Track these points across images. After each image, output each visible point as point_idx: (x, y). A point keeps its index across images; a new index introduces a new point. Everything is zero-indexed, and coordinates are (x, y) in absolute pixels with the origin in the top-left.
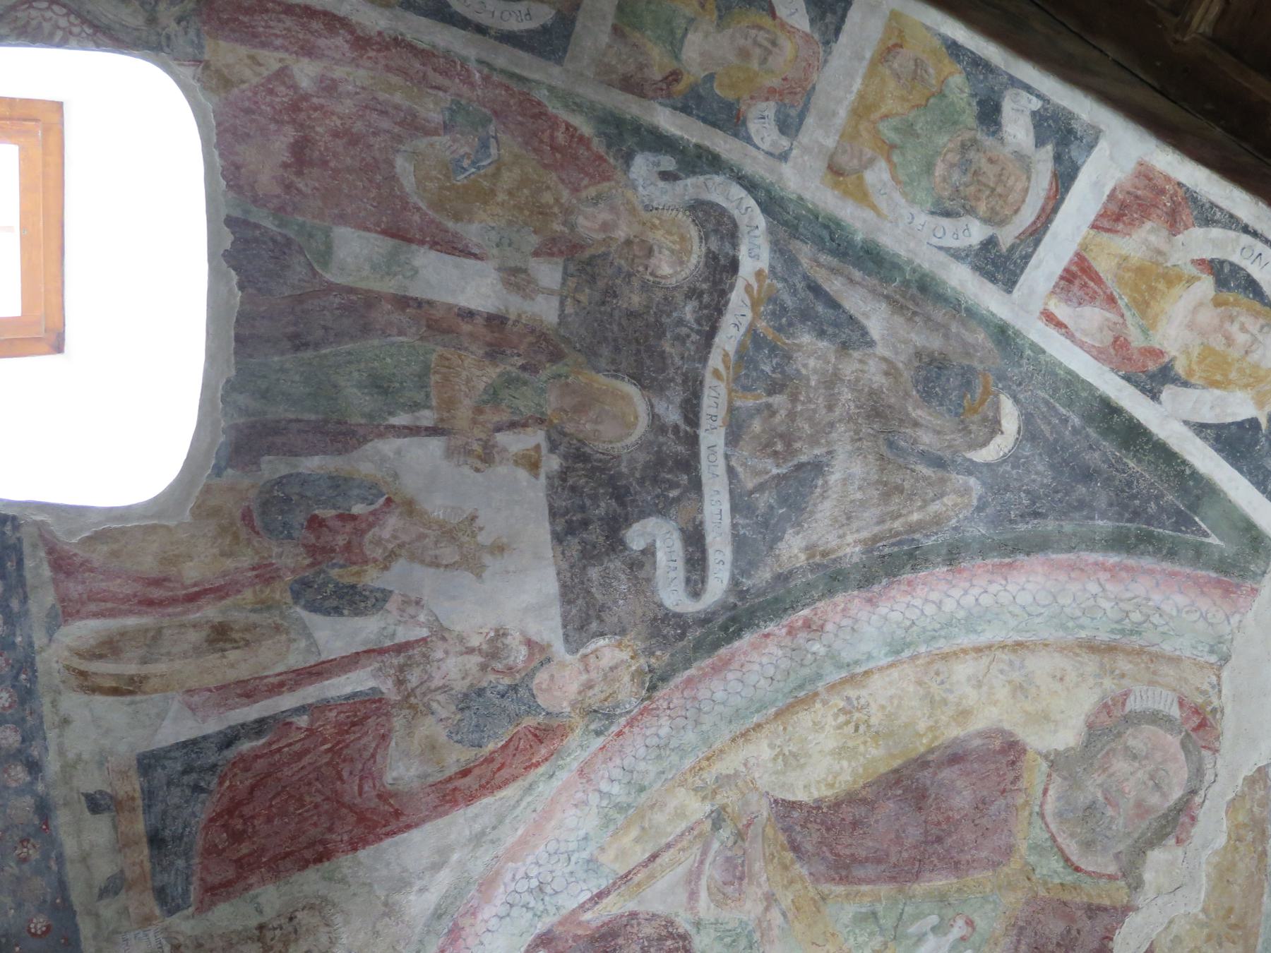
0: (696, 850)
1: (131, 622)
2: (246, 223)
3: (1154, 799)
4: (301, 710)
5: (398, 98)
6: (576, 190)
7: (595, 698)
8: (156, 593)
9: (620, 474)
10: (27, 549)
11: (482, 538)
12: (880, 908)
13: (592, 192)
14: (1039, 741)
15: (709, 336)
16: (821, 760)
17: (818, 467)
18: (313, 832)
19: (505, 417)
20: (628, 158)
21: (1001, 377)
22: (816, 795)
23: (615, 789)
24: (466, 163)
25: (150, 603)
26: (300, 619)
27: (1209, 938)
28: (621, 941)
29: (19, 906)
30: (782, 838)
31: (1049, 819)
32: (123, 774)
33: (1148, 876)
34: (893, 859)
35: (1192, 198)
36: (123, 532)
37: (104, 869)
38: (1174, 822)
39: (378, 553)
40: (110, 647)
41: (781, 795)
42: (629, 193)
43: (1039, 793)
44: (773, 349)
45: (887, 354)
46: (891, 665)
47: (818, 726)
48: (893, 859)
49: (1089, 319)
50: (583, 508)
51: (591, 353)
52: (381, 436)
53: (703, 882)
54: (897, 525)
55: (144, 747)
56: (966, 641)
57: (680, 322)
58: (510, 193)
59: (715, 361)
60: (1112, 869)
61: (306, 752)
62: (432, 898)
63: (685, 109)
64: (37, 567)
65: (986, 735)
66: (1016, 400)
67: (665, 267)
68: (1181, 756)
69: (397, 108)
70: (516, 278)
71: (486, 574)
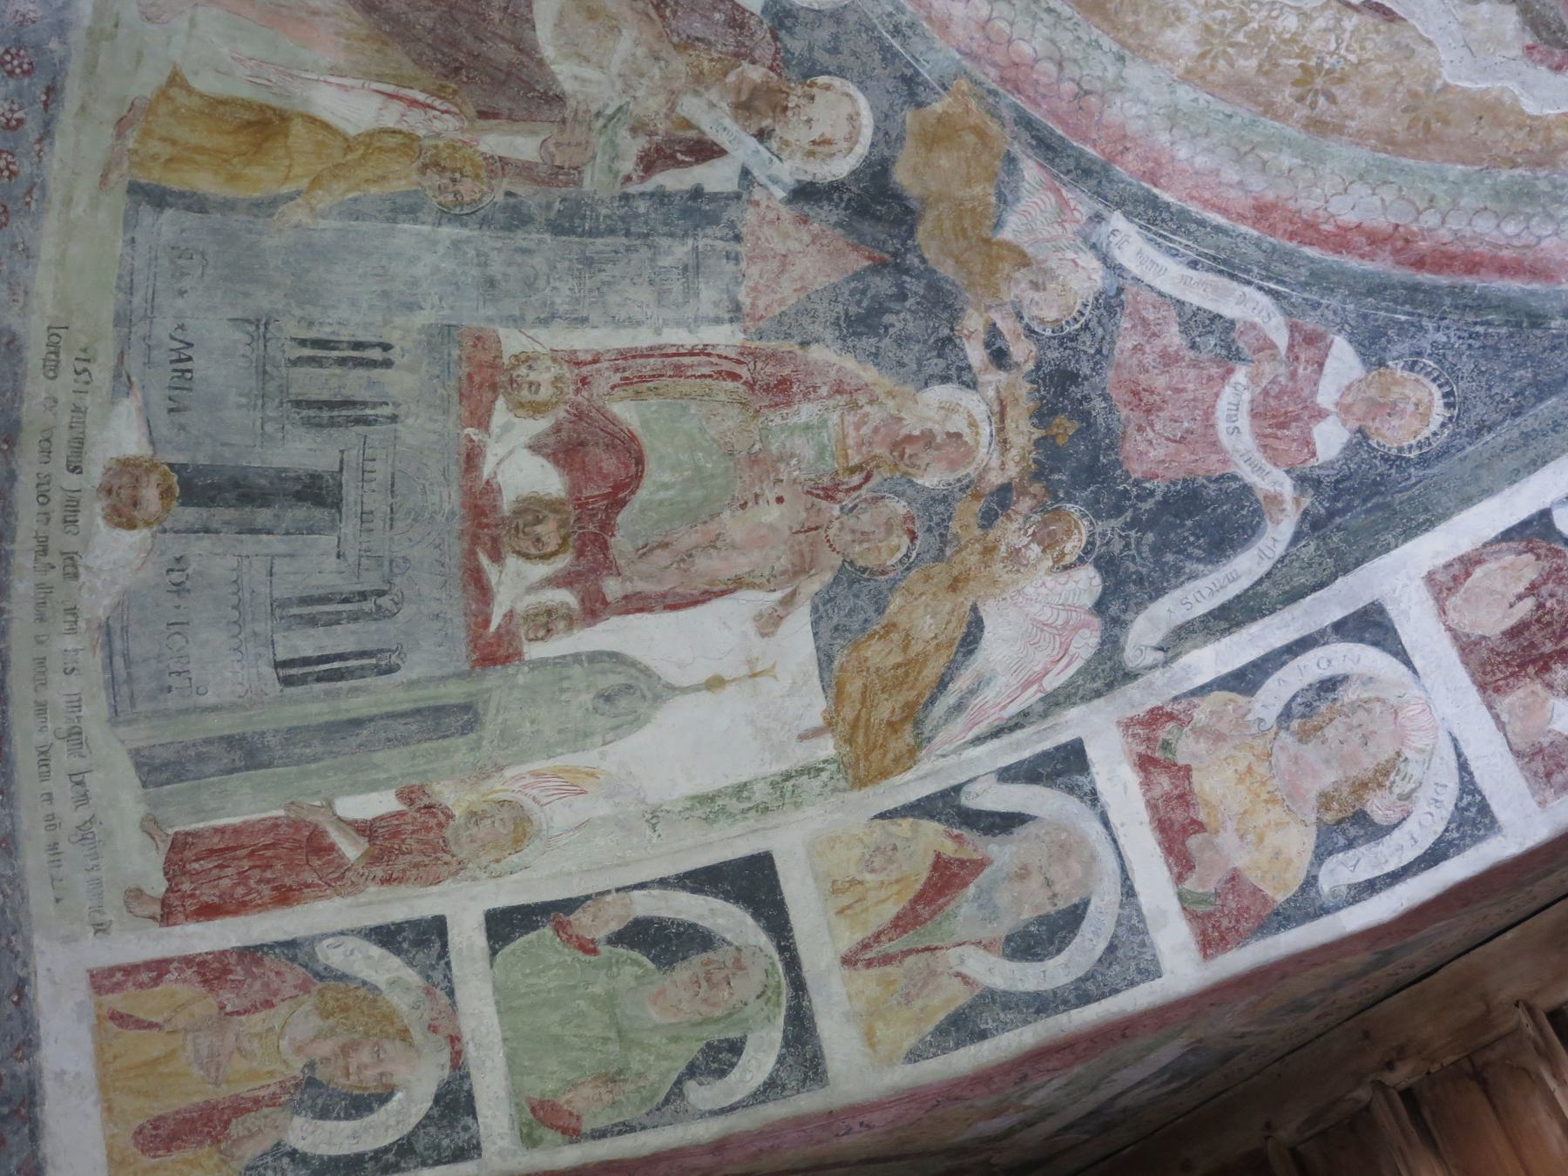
27: (1414, 95)
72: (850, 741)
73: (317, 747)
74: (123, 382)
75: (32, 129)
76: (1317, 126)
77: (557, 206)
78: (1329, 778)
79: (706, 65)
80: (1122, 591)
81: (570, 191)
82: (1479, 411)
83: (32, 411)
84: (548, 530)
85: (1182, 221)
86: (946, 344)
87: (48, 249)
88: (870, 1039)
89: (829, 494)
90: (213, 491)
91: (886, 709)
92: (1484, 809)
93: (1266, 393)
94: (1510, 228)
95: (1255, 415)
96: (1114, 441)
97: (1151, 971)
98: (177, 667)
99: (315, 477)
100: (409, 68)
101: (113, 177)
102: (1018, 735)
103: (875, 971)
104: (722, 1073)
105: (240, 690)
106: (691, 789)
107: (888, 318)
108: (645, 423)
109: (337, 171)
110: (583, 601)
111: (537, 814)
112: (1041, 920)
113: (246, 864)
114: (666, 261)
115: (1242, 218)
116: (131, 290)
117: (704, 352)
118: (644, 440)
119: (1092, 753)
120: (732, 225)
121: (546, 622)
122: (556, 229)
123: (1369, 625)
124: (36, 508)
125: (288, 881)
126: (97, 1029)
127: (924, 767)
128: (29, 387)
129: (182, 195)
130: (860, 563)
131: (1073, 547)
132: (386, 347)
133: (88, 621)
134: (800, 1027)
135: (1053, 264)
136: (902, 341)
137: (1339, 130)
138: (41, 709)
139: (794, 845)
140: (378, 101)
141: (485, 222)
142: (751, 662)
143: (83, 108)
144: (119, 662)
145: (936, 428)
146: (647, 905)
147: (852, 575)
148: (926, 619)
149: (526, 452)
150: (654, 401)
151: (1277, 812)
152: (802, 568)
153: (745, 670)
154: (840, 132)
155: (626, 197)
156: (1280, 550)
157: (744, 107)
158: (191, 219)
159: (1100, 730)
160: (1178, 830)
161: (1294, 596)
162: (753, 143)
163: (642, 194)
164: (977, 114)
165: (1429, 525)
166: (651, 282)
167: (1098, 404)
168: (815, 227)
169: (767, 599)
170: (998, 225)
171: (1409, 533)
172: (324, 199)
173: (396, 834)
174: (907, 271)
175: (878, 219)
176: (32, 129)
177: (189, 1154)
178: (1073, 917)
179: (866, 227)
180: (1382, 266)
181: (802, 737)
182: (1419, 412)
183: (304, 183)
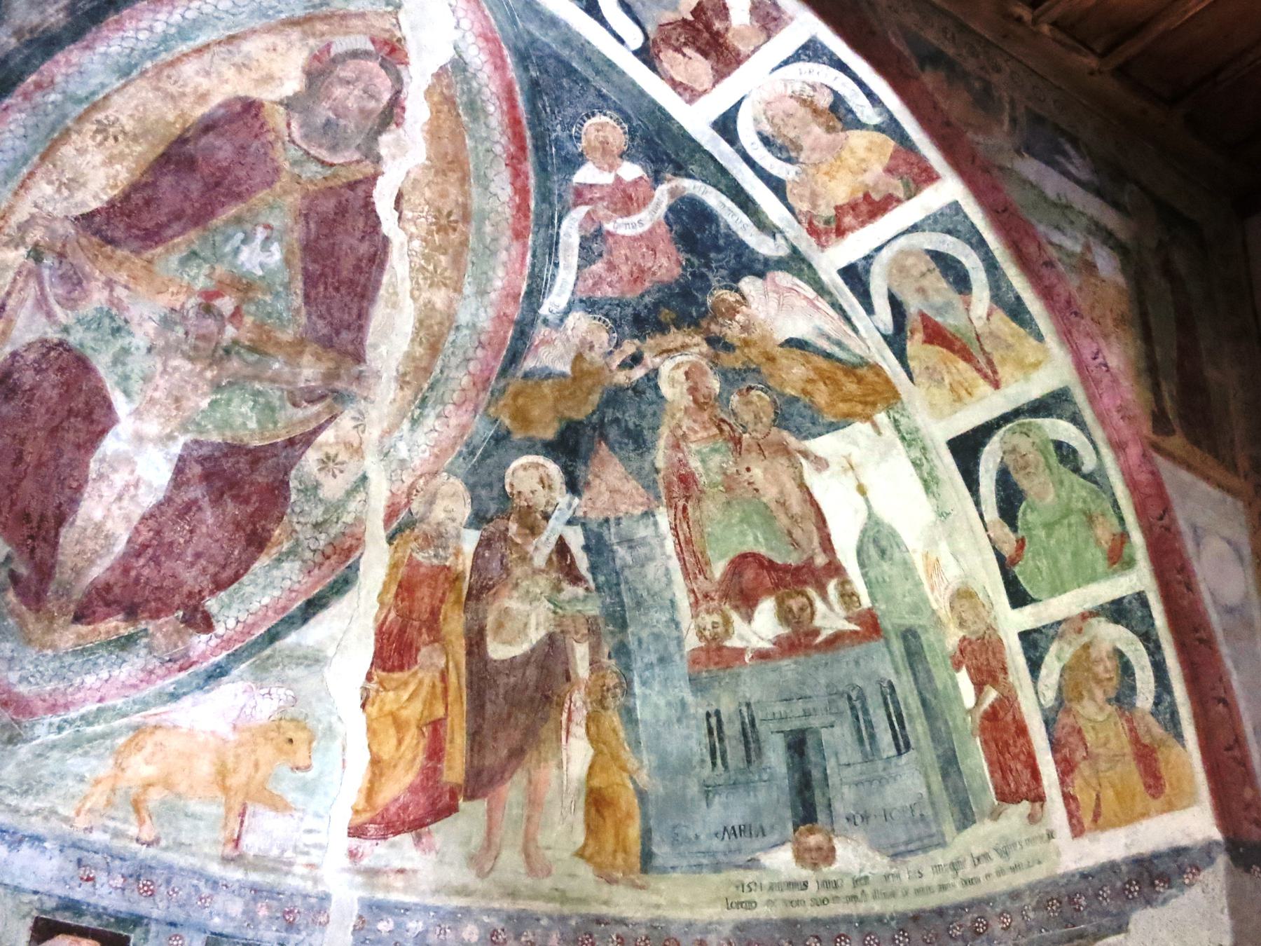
0: (33, 284)
3: (372, 104)
12: (195, 247)
14: (267, 95)
22: (106, 198)
27: (437, 173)
28: (16, 376)
30: (95, 239)
31: (299, 141)
33: (383, 151)
34: (189, 211)
38: (392, 114)
41: (76, 212)
43: (283, 126)
46: (124, 86)
47: (81, 152)
48: (189, 211)
53: (52, 300)
56: (184, 48)
60: (357, 156)
65: (226, 105)
68: (383, 72)
72: (874, 404)
73: (940, 724)
74: (752, 864)
75: (622, 930)
77: (611, 628)
78: (817, 130)
79: (514, 556)
80: (747, 264)
81: (601, 621)
82: (591, 98)
83: (775, 913)
84: (795, 603)
85: (534, 276)
86: (636, 389)
87: (685, 915)
88: (1036, 365)
89: (738, 442)
90: (807, 804)
91: (851, 387)
92: (805, 47)
93: (615, 211)
94: (491, 109)
95: (629, 214)
96: (664, 287)
97: (955, 207)
98: (909, 814)
99: (789, 747)
100: (551, 724)
101: (639, 882)
102: (845, 307)
103: (999, 370)
104: (1074, 451)
105: (917, 773)
107: (631, 425)
108: (722, 557)
109: (615, 758)
110: (832, 577)
111: (954, 585)
112: (945, 275)
113: (1007, 756)
114: (629, 560)
115: (525, 245)
116: (700, 865)
117: (675, 529)
118: (731, 555)
119: (843, 264)
120: (600, 525)
121: (848, 597)
122: (624, 626)
123: (726, 126)
124: (831, 905)
125: (1013, 729)
126: (1103, 829)
128: (762, 916)
129: (643, 844)
130: (773, 416)
131: (731, 297)
132: (708, 715)
133: (891, 867)
135: (577, 341)
136: (642, 415)
137: (465, 207)
138: (943, 887)
140: (571, 740)
141: (628, 668)
142: (845, 471)
143: (606, 903)
144: (912, 847)
145: (685, 386)
146: (992, 513)
147: (781, 419)
148: (795, 373)
149: (754, 624)
150: (709, 553)
151: (845, 154)
152: (785, 450)
153: (850, 473)
155: (598, 588)
156: (699, 183)
157: (533, 530)
158: (656, 837)
159: (831, 260)
160: (872, 207)
161: (723, 171)
162: (552, 522)
163: (595, 580)
164: (506, 400)
165: (661, 109)
166: (643, 566)
167: (647, 299)
168: (590, 477)
170: (563, 375)
171: (669, 118)
172: (632, 764)
173: (979, 670)
174: (602, 420)
175: (577, 443)
176: (622, 930)
177: (1162, 765)
178: (937, 256)
180: (529, 167)
181: (879, 433)
182: (603, 128)
183: (625, 775)
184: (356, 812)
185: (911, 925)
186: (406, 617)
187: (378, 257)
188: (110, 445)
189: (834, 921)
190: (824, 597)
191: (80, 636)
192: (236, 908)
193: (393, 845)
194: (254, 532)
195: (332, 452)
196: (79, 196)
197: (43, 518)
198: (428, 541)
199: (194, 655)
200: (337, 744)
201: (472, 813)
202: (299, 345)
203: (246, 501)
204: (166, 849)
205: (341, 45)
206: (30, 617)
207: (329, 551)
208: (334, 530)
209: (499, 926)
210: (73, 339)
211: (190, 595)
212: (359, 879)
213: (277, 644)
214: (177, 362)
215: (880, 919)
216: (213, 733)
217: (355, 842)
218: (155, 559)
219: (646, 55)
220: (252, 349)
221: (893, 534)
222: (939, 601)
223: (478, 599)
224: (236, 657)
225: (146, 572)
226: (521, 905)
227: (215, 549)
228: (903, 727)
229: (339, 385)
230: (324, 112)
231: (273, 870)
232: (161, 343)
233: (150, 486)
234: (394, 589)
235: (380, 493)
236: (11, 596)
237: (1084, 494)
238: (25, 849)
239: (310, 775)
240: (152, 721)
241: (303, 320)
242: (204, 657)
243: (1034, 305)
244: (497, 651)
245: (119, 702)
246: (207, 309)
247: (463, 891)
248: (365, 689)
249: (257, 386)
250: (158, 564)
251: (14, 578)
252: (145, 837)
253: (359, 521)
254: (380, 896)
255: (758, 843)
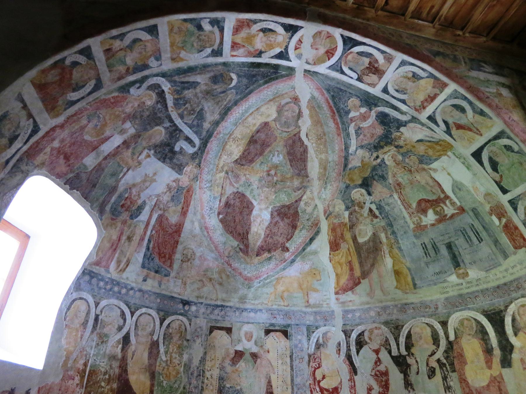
1: (117, 255)
2: (68, 180)
3: (294, 114)
4: (152, 231)
5: (76, 127)
6: (122, 106)
7: (192, 177)
8: (114, 247)
9: (166, 142)
10: (91, 269)
11: (150, 176)
12: (262, 161)
13: (125, 103)
14: (269, 120)
15: (166, 107)
16: (236, 150)
17: (202, 109)
18: (173, 242)
19: (138, 154)
20: (128, 91)
21: (228, 71)
23: (207, 185)
24: (97, 124)
25: (115, 249)
26: (137, 221)
29: (154, 303)
30: (239, 166)
32: (143, 272)
35: (251, 20)
36: (99, 247)
37: (156, 284)
38: (300, 115)
39: (136, 197)
40: (119, 262)
41: (233, 161)
42: (133, 97)
44: (180, 99)
45: (204, 82)
47: (231, 146)
49: (241, 51)
50: (164, 153)
51: (145, 130)
52: (120, 181)
54: (223, 107)
55: (140, 265)
56: (247, 115)
57: (159, 109)
58: (110, 119)
59: (170, 109)
60: (294, 128)
61: (159, 235)
62: (198, 228)
63: (134, 73)
64: (96, 269)
65: (260, 125)
66: (233, 73)
67: (149, 103)
69: (77, 129)
70: (122, 132)
71: (157, 180)
72: (446, 151)
74: (445, 281)
75: (413, 306)
76: (325, 135)
78: (410, 83)
80: (400, 124)
82: (348, 95)
83: (456, 293)
84: (438, 209)
85: (346, 144)
86: (380, 165)
87: (430, 298)
88: (492, 126)
89: (411, 171)
90: (456, 262)
91: (438, 148)
92: (401, 63)
94: (324, 106)
95: (366, 121)
97: (456, 91)
99: (447, 247)
100: (380, 256)
104: (511, 147)
106: (467, 171)
108: (414, 202)
111: (484, 193)
112: (457, 110)
114: (389, 209)
116: (430, 284)
117: (399, 198)
118: (417, 201)
119: (427, 116)
121: (453, 204)
122: (392, 226)
123: (385, 90)
127: (445, 139)
131: (398, 134)
132: (422, 244)
134: (497, 137)
135: (361, 157)
138: (504, 277)
139: (468, 151)
141: (396, 237)
146: (489, 170)
147: (421, 162)
148: (421, 149)
150: (410, 202)
152: (424, 169)
154: (359, 194)
155: (383, 218)
157: (362, 208)
158: (416, 279)
159: (423, 116)
160: (432, 98)
161: (387, 102)
164: (346, 176)
165: (367, 92)
167: (376, 141)
169: (432, 172)
170: (360, 167)
171: (369, 93)
172: (404, 261)
173: (498, 214)
175: (367, 182)
178: (454, 106)
179: (369, 183)
182: (353, 101)
184: (335, 288)
185: (497, 290)
186: (335, 237)
187: (305, 151)
188: (254, 213)
189: (474, 292)
190: (446, 205)
191: (259, 260)
192: (312, 318)
193: (347, 295)
194: (293, 225)
195: (307, 201)
196: (233, 156)
197: (243, 233)
198: (336, 217)
199: (286, 258)
200: (326, 272)
201: (365, 283)
202: (292, 178)
203: (289, 218)
204: (291, 307)
205: (283, 102)
206: (246, 257)
207: (312, 225)
208: (312, 220)
209: (379, 310)
210: (240, 190)
211: (282, 244)
212: (340, 305)
213: (305, 251)
214: (265, 189)
215: (487, 289)
216: (296, 276)
217: (337, 296)
218: (271, 237)
219: (359, 79)
220: (282, 181)
221: (461, 183)
222: (481, 198)
223: (352, 228)
224: (296, 256)
225: (270, 241)
226: (384, 304)
227: (285, 231)
228: (479, 235)
229: (304, 184)
230: (283, 119)
231: (319, 307)
232: (260, 186)
233: (266, 220)
234: (330, 231)
235: (321, 208)
236: (241, 254)
237: (517, 157)
238: (258, 313)
239: (322, 281)
240: (281, 276)
241: (292, 171)
242: (289, 258)
243: (486, 110)
244: (361, 240)
245: (272, 273)
246: (269, 175)
247: (368, 303)
248: (330, 257)
249: (285, 190)
250: (272, 238)
251: (240, 249)
252: (286, 304)
253: (318, 216)
254: (347, 308)
255: (445, 275)
